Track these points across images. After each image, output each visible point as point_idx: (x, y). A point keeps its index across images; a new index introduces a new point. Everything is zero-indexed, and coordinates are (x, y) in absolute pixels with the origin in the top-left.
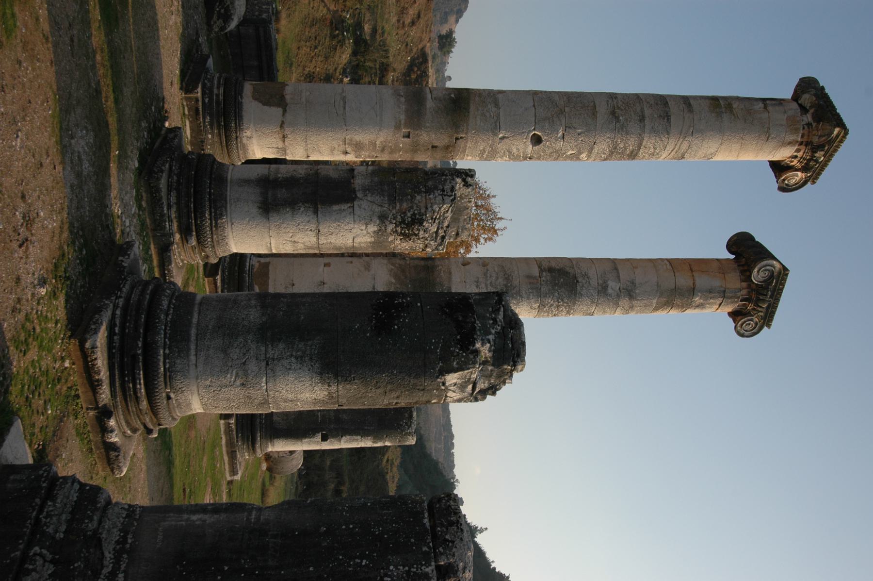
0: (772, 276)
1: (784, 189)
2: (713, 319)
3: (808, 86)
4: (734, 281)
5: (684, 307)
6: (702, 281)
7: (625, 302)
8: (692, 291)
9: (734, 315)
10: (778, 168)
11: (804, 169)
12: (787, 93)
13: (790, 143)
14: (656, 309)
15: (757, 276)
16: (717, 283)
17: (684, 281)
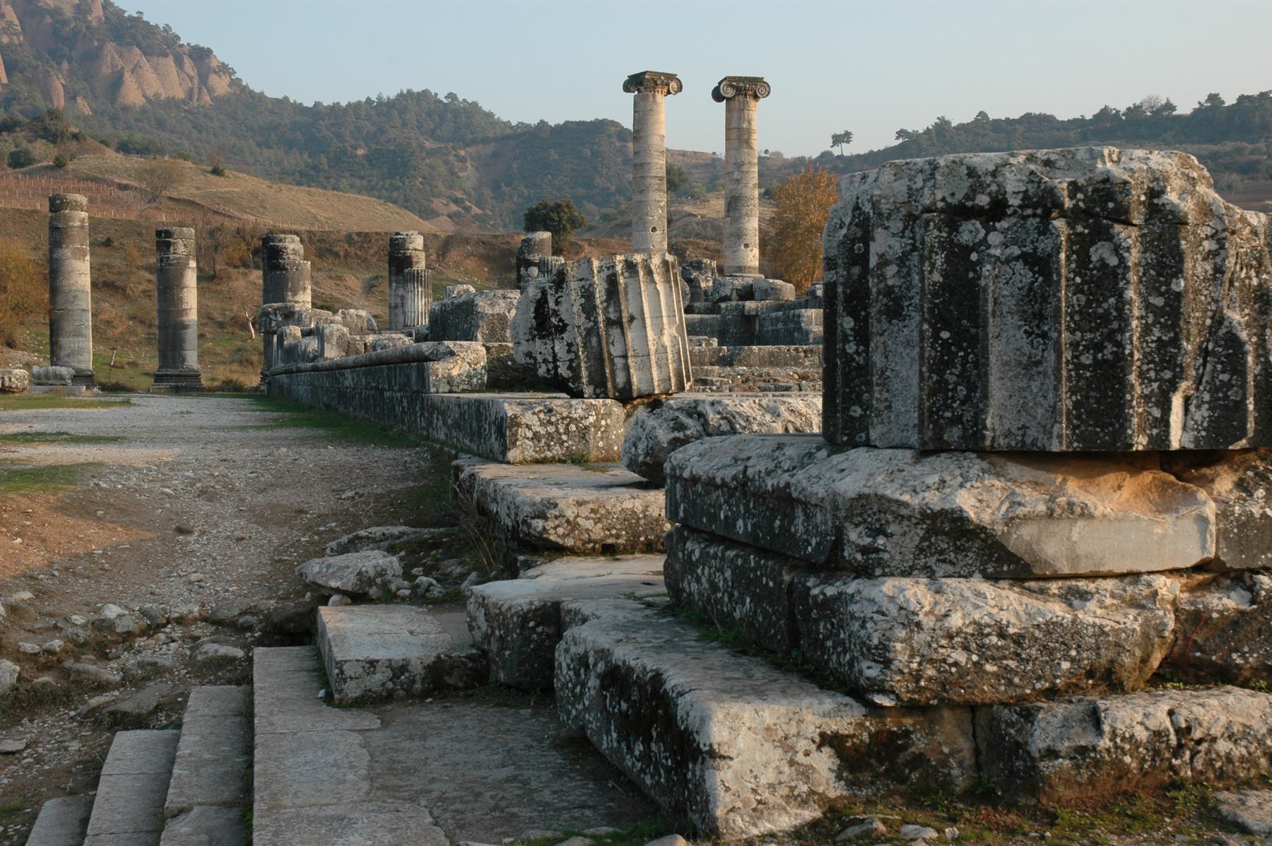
0: (731, 86)
1: (680, 88)
2: (760, 113)
3: (627, 88)
4: (735, 104)
5: (749, 132)
6: (734, 125)
7: (745, 168)
8: (739, 129)
9: (756, 97)
10: (669, 93)
11: (668, 85)
12: (630, 97)
13: (654, 96)
14: (751, 148)
15: (730, 93)
16: (735, 115)
17: (734, 135)
